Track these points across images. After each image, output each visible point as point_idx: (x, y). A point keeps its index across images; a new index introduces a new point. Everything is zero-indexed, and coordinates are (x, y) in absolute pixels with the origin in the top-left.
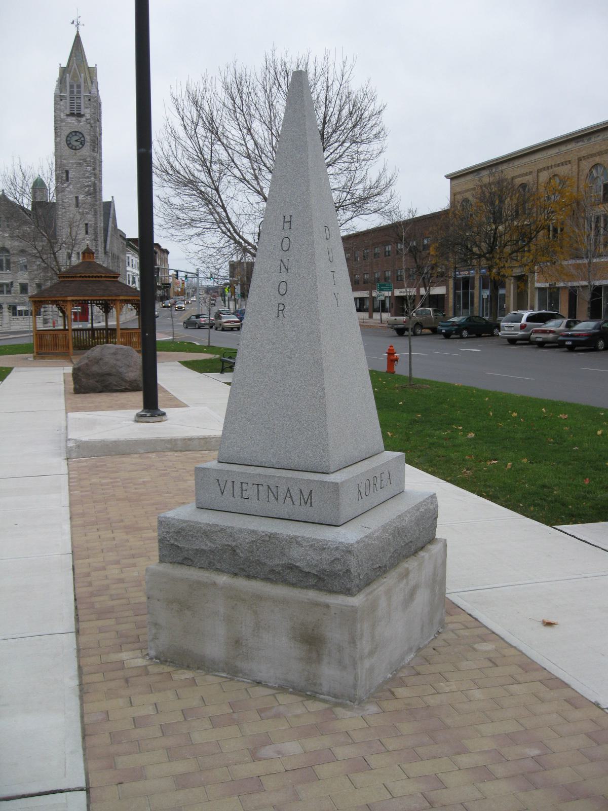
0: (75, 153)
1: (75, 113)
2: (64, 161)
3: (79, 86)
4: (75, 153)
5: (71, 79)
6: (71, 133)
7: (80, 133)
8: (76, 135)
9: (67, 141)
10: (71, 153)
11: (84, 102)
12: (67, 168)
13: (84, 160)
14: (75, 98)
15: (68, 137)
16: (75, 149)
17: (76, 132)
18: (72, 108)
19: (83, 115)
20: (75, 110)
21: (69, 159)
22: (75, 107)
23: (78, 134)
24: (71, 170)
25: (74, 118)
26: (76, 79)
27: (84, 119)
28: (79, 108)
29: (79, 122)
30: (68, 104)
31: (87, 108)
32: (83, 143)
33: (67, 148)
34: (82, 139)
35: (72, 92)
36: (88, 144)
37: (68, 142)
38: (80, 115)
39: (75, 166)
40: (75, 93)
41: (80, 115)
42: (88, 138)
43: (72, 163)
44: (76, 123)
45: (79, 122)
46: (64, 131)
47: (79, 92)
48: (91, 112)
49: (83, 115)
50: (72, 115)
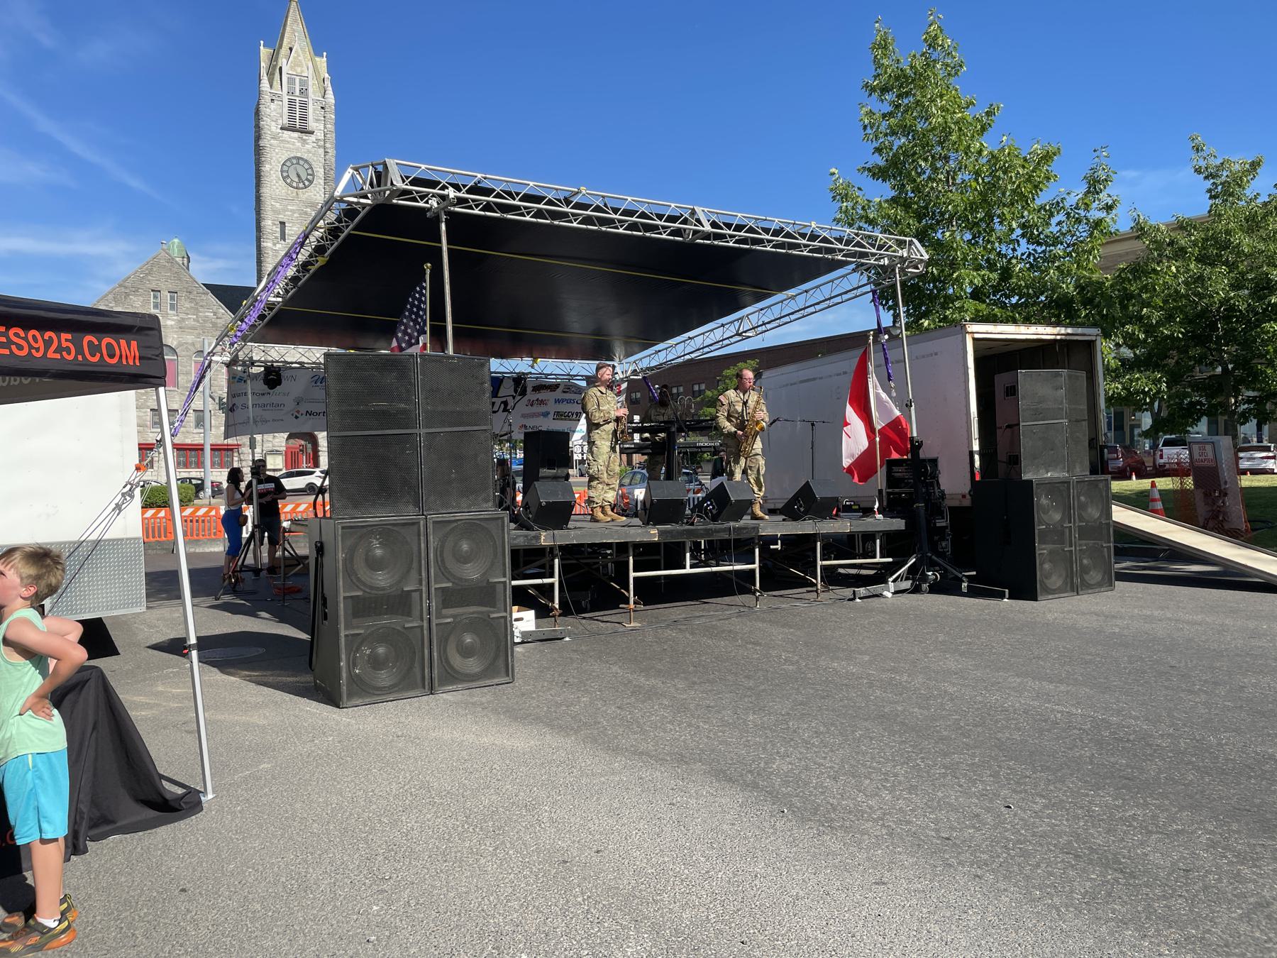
0: (297, 194)
1: (298, 126)
2: (278, 205)
3: (304, 83)
4: (297, 194)
5: (292, 68)
6: (289, 159)
7: (306, 161)
8: (298, 164)
9: (282, 171)
10: (289, 192)
11: (314, 110)
12: (282, 218)
14: (297, 101)
15: (283, 164)
16: (297, 188)
17: (299, 158)
18: (291, 117)
19: (312, 133)
20: (298, 121)
21: (286, 202)
22: (298, 115)
23: (302, 162)
24: (289, 223)
25: (296, 135)
26: (299, 70)
27: (313, 138)
28: (304, 118)
29: (304, 142)
30: (286, 110)
31: (317, 120)
32: (311, 182)
33: (281, 182)
34: (310, 171)
37: (285, 174)
38: (305, 131)
39: (295, 215)
40: (297, 93)
41: (305, 131)
43: (291, 211)
44: (300, 144)
45: (304, 142)
46: (277, 154)
47: (303, 92)
48: (325, 128)
49: (312, 133)
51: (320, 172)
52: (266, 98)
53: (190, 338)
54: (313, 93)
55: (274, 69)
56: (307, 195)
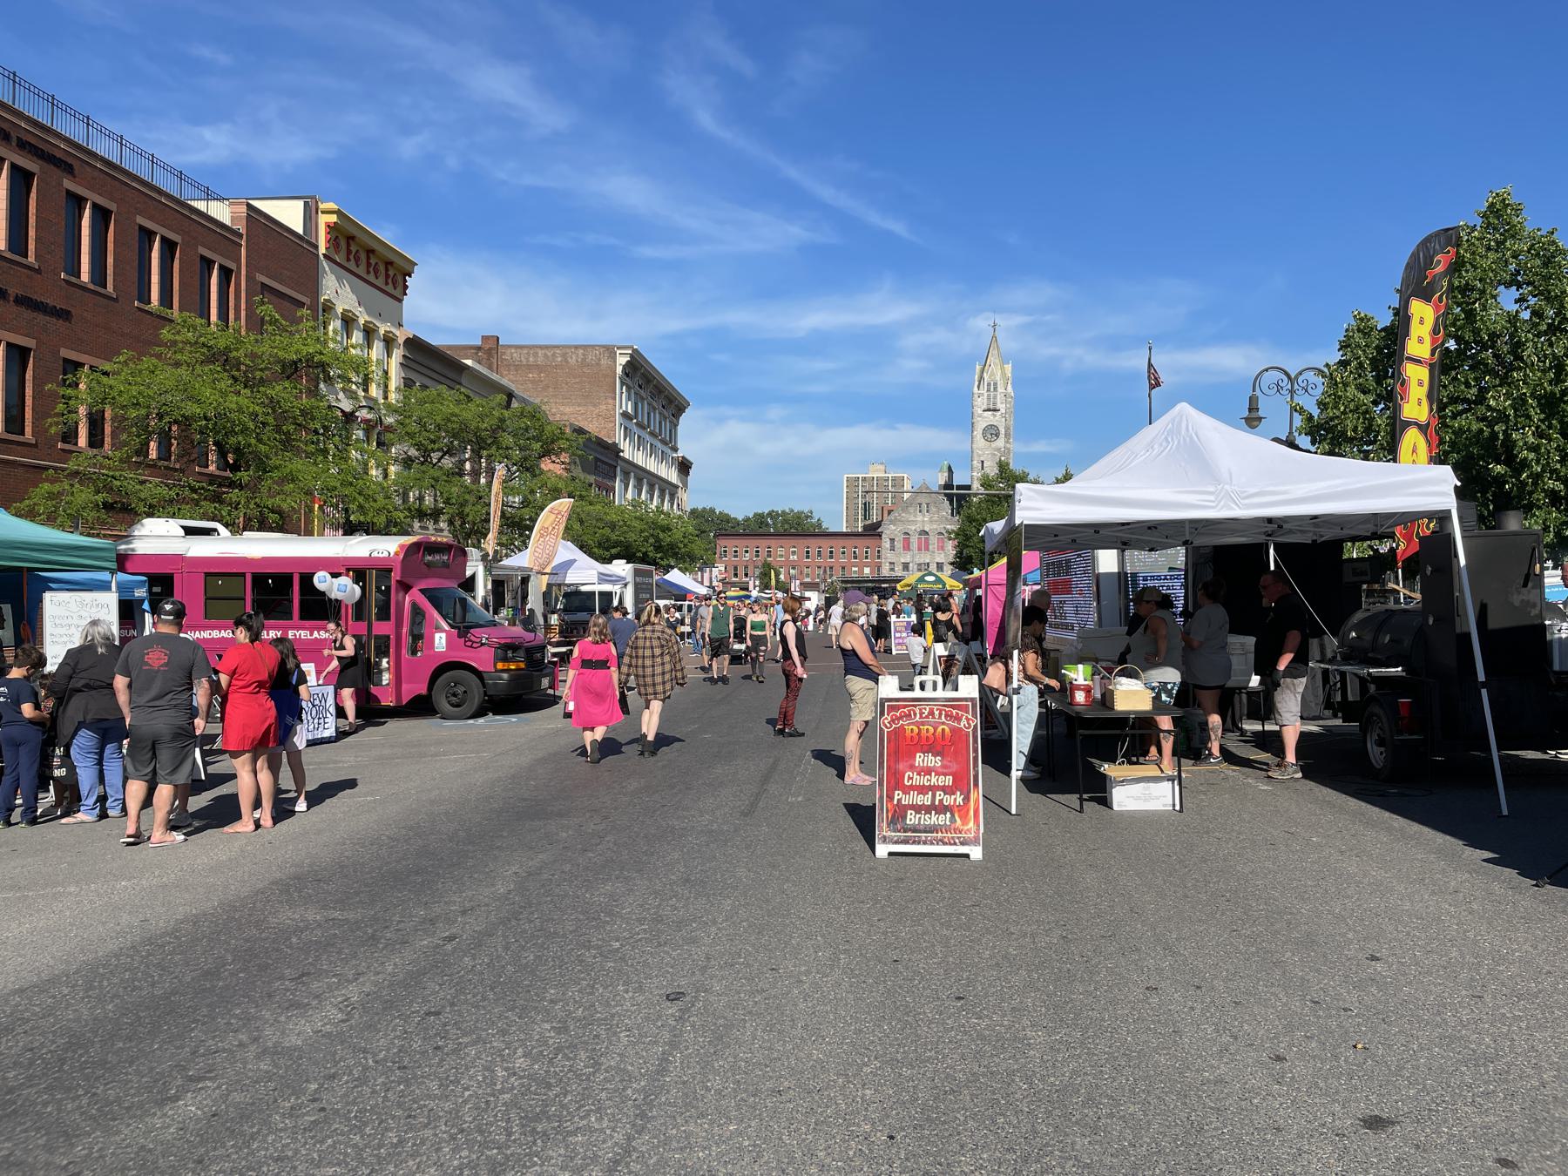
3: (995, 384)
12: (982, 459)
13: (999, 450)
27: (999, 413)
29: (995, 416)
32: (997, 435)
35: (988, 390)
36: (1002, 435)
42: (1002, 431)
45: (995, 416)
47: (995, 389)
50: (989, 410)
51: (1002, 431)
52: (976, 396)
53: (935, 526)
54: (1001, 389)
55: (981, 378)
56: (994, 445)
